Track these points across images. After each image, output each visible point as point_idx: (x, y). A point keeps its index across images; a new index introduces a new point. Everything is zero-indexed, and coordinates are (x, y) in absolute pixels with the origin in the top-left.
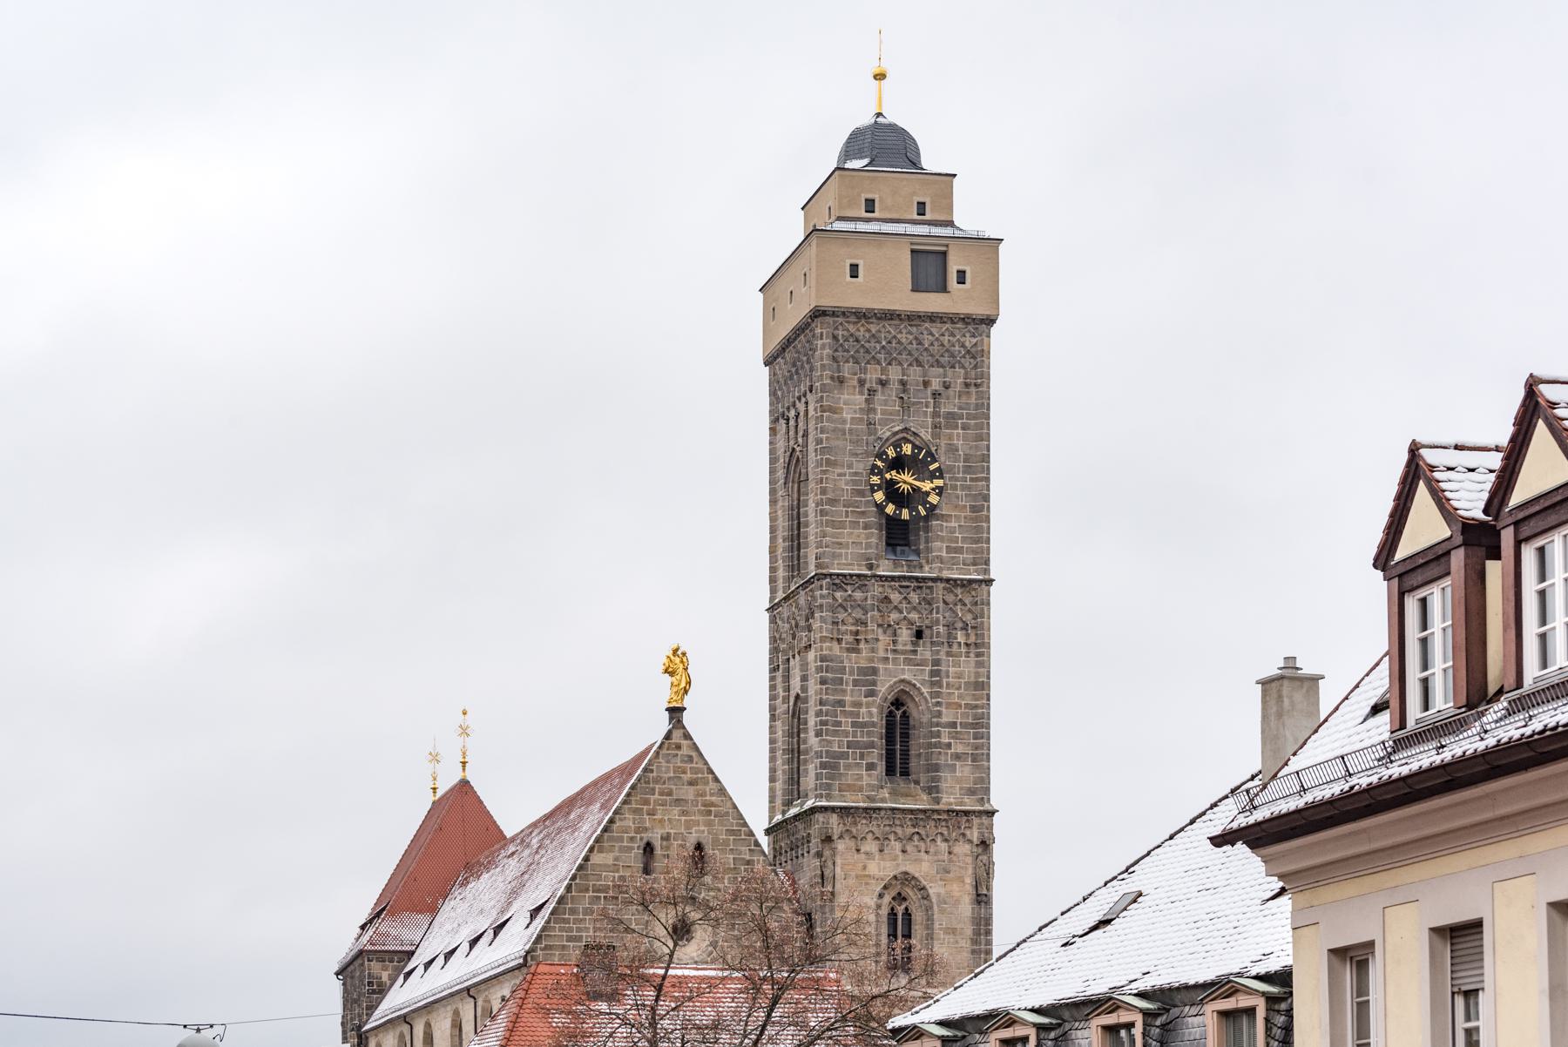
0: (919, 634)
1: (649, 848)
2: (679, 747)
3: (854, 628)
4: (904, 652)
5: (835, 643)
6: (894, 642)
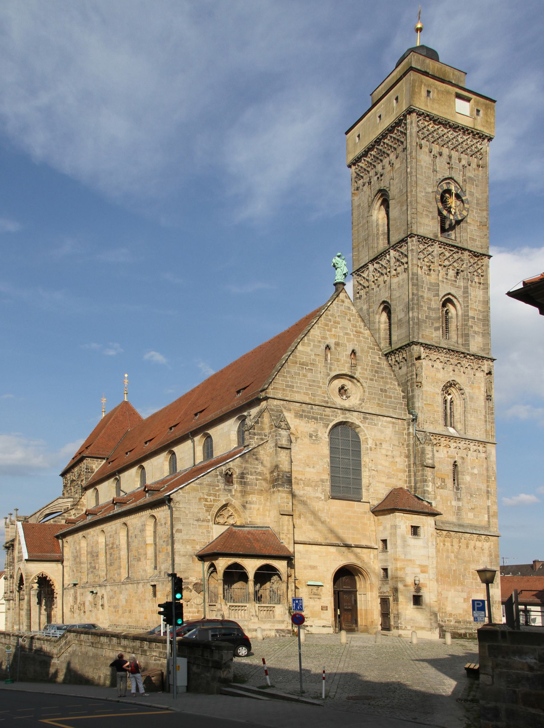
1: (328, 347)
2: (343, 301)
3: (428, 264)
4: (451, 281)
5: (419, 269)
6: (447, 274)
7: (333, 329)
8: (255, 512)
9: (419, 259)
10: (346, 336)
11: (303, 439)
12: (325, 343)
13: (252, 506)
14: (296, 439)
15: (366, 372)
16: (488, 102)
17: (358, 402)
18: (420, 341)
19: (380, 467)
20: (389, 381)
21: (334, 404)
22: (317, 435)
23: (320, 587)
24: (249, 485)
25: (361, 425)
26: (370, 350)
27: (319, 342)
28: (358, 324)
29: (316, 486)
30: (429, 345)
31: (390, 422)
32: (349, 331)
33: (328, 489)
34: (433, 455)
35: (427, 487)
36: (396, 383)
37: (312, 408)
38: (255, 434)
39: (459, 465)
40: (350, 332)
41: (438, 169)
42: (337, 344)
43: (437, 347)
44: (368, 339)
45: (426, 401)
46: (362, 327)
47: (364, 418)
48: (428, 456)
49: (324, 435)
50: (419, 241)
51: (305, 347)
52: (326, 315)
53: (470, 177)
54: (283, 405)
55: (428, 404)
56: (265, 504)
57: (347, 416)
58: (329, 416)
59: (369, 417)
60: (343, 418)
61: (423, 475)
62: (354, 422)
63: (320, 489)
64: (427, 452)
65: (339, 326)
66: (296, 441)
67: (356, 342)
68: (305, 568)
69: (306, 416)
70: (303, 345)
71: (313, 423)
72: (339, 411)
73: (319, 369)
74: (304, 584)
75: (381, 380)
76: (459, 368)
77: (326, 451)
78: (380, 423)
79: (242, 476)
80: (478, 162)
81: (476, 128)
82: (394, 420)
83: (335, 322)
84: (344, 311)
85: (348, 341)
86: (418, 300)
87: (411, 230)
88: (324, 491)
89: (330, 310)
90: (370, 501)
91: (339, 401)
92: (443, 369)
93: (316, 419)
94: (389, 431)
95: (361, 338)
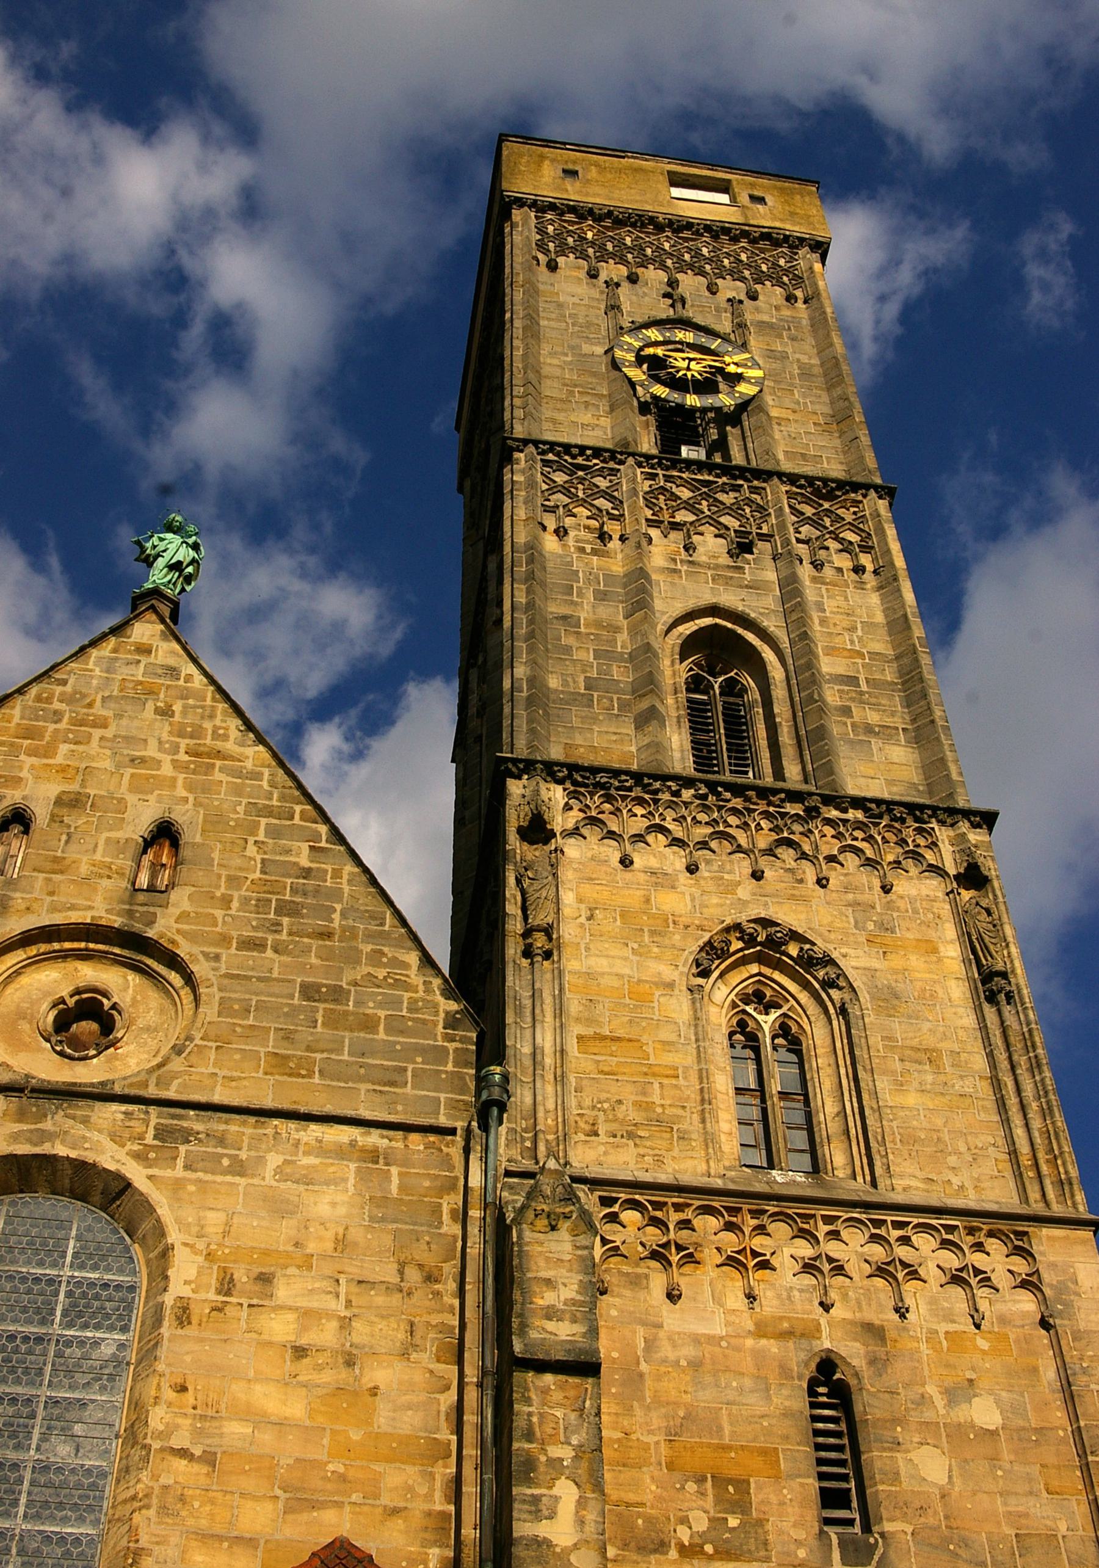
7: (64, 748)
15: (219, 913)
19: (236, 1430)
20: (368, 948)
25: (137, 1175)
31: (341, 1153)
39: (853, 1382)
42: (70, 802)
47: (162, 1133)
59: (198, 1127)
65: (97, 733)
67: (181, 792)
75: (315, 943)
78: (274, 1160)
82: (375, 1139)
94: (334, 1203)
95: (218, 776)
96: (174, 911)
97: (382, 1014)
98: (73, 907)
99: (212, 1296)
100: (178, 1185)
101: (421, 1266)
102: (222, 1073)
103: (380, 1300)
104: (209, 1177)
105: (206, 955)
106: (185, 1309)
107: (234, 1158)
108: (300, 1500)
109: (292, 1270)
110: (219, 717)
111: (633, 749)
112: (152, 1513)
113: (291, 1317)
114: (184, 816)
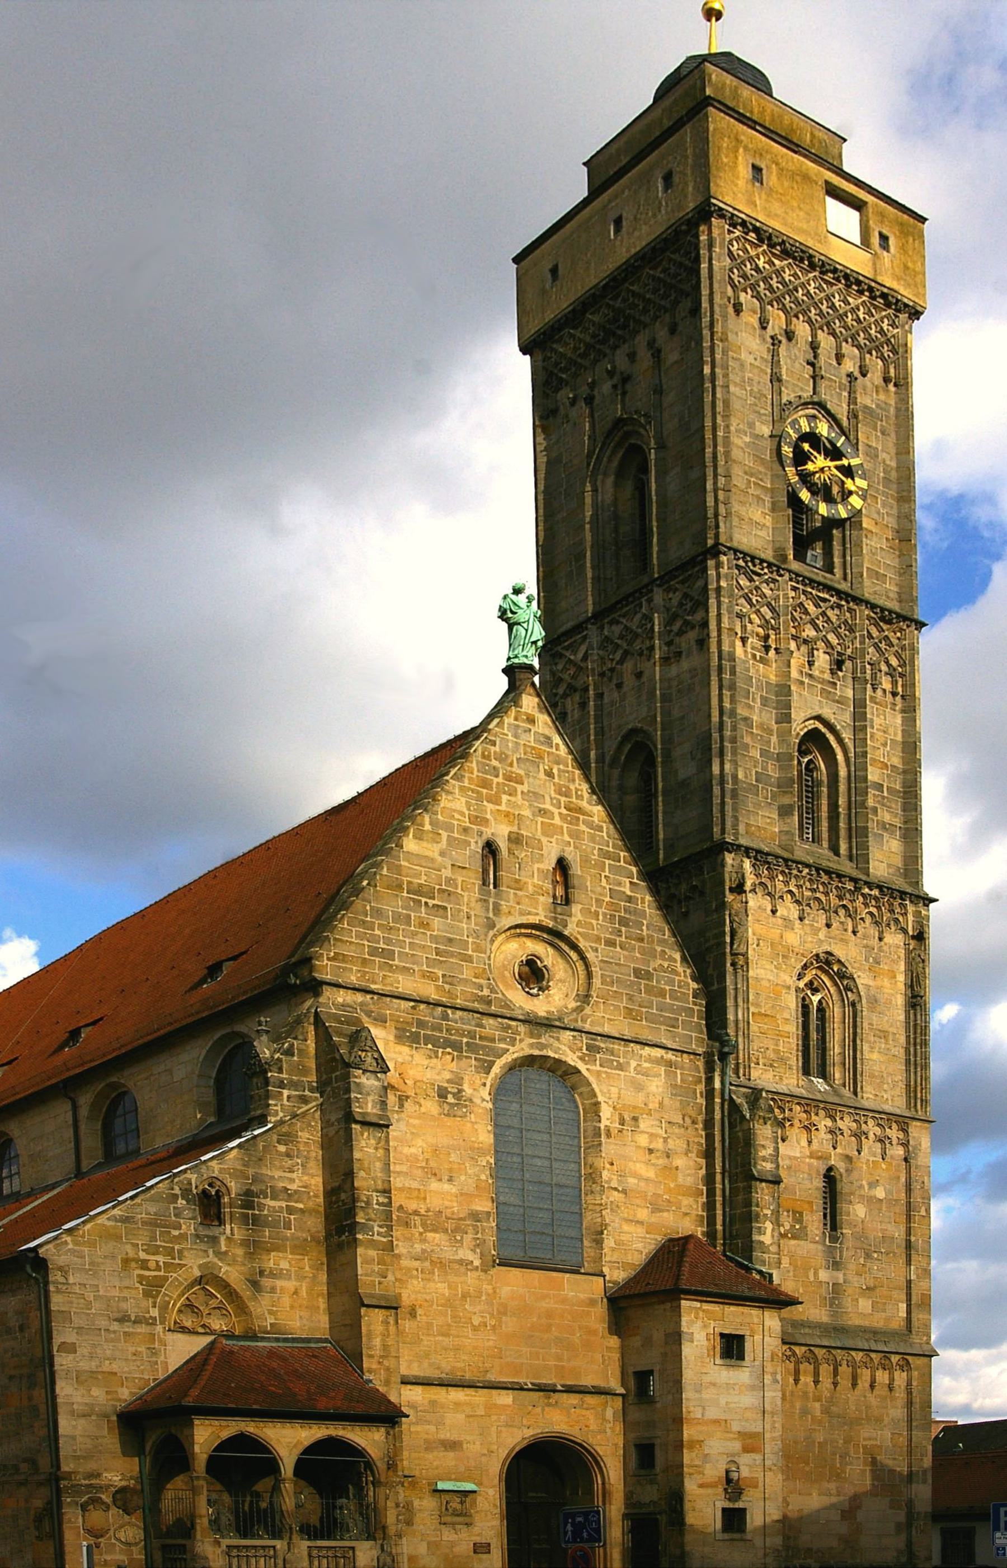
0: (839, 664)
1: (490, 849)
5: (738, 643)
6: (811, 664)
7: (505, 798)
8: (286, 1301)
9: (740, 616)
10: (540, 819)
11: (422, 1101)
12: (480, 834)
13: (279, 1283)
14: (402, 1100)
15: (594, 922)
16: (906, 217)
17: (572, 1005)
18: (743, 841)
19: (632, 1181)
20: (659, 949)
21: (507, 1006)
22: (460, 1091)
23: (471, 1496)
24: (267, 1224)
25: (582, 1067)
26: (607, 862)
27: (466, 830)
28: (572, 787)
29: (456, 1230)
30: (768, 854)
32: (548, 806)
33: (491, 1239)
34: (777, 1149)
35: (760, 1233)
36: (677, 956)
37: (445, 1017)
38: (281, 1085)
40: (551, 808)
41: (784, 377)
42: (515, 839)
43: (786, 860)
44: (600, 829)
45: (757, 1005)
46: (586, 795)
47: (589, 1047)
48: (763, 1153)
49: (479, 1091)
50: (738, 567)
51: (425, 844)
52: (484, 756)
53: (866, 407)
54: (362, 1004)
55: (760, 1014)
56: (314, 1277)
57: (543, 1040)
58: (493, 1040)
59: (602, 1045)
60: (531, 1046)
61: (748, 1203)
62: (564, 1058)
63: (468, 1238)
64: (760, 1141)
65: (520, 788)
66: (401, 1106)
67: (567, 838)
68: (429, 1446)
69: (428, 1040)
70: (419, 837)
71: (449, 1057)
72: (522, 1028)
73: (465, 908)
74: (426, 1489)
75: (638, 944)
76: (843, 919)
77: (485, 1136)
78: (633, 1064)
79: (248, 1199)
80: (886, 370)
81: (879, 279)
82: (670, 1056)
83: (509, 778)
84: (533, 748)
85: (544, 834)
86: (734, 728)
87: (717, 535)
88: (479, 1244)
89: (494, 744)
90: (606, 1270)
91: (519, 999)
92: (801, 919)
93: (456, 1046)
94: (657, 1086)
95: (583, 827)
96: (575, 919)
97: (668, 988)
98: (529, 913)
99: (617, 1125)
100: (599, 1073)
101: (690, 1117)
102: (607, 1016)
103: (677, 1131)
104: (609, 1071)
105: (591, 947)
106: (609, 1130)
107: (618, 1061)
108: (656, 1209)
109: (644, 1116)
110: (577, 781)
111: (777, 830)
112: (608, 1211)
113: (646, 1136)
114: (572, 855)
